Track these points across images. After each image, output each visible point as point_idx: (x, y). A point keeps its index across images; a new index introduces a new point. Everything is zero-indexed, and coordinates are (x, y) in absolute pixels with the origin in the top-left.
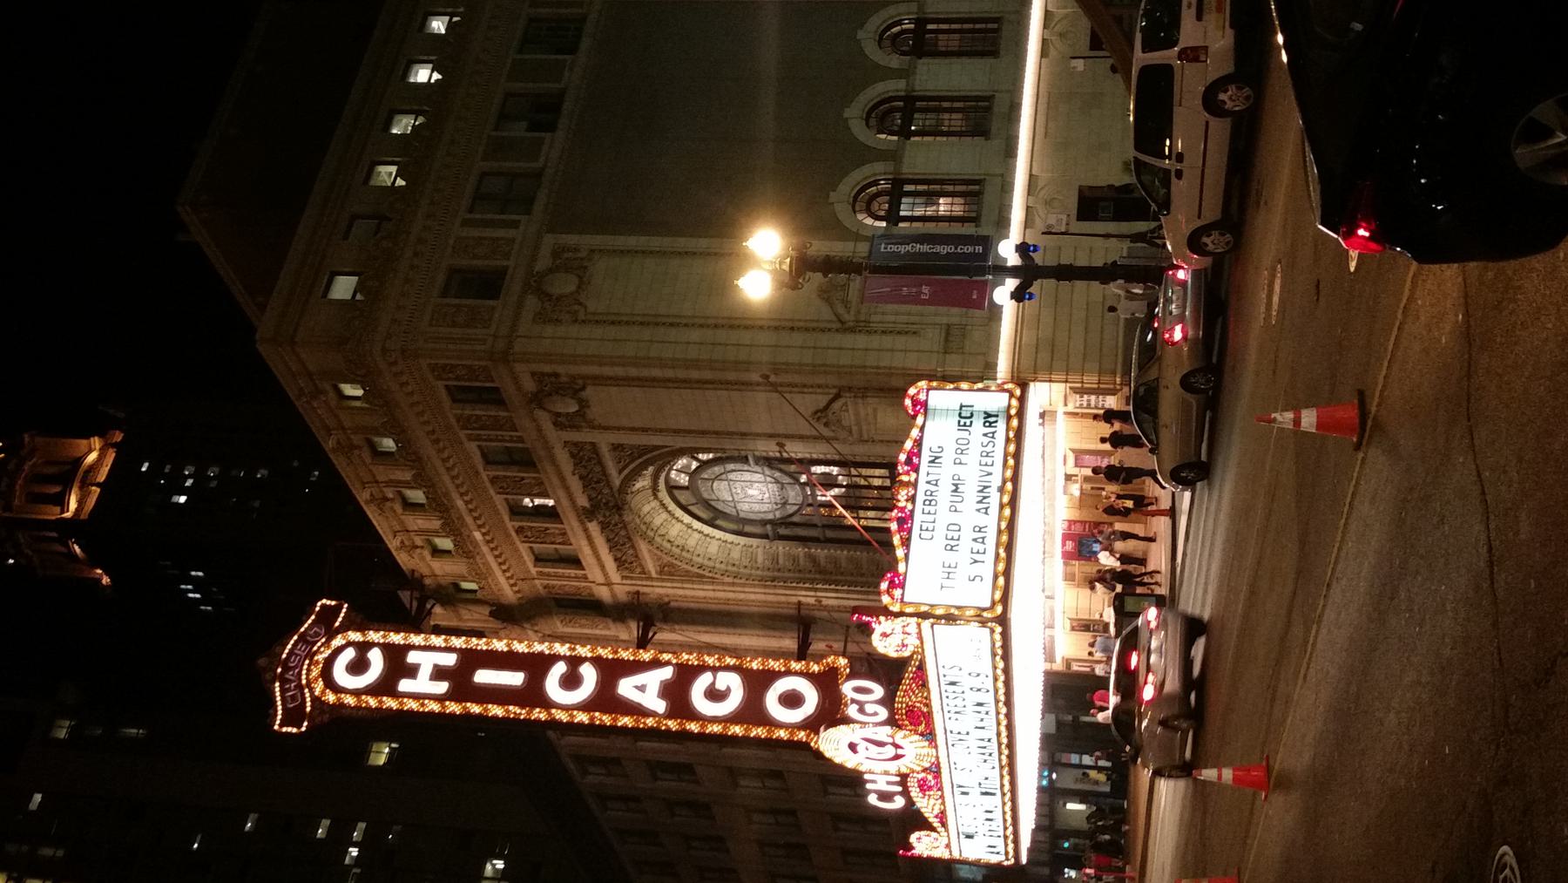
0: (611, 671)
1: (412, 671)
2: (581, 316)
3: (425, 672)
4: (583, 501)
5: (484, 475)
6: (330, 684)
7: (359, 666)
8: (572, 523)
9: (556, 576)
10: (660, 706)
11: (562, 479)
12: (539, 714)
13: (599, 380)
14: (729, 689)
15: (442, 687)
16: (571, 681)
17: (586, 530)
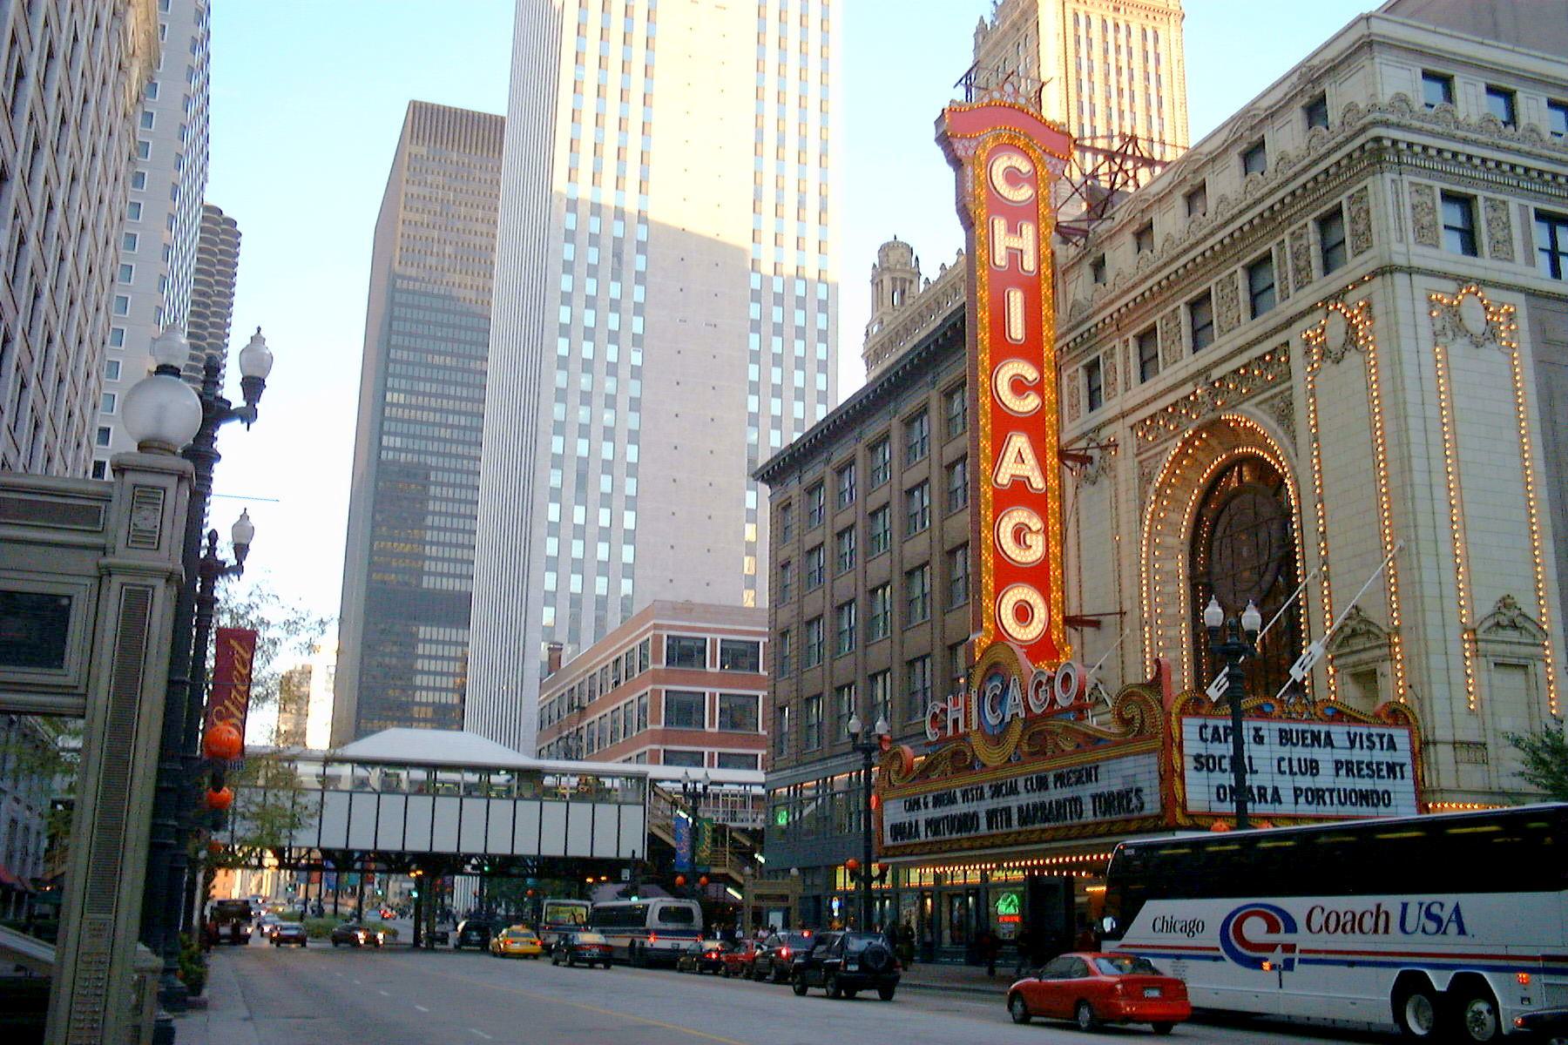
0: (1033, 426)
1: (1013, 229)
2: (1441, 340)
3: (1015, 243)
4: (1216, 374)
5: (1238, 267)
6: (992, 154)
7: (1013, 177)
8: (1190, 363)
10: (1004, 479)
11: (1241, 350)
12: (984, 358)
15: (1001, 259)
16: (1019, 386)
17: (1184, 382)
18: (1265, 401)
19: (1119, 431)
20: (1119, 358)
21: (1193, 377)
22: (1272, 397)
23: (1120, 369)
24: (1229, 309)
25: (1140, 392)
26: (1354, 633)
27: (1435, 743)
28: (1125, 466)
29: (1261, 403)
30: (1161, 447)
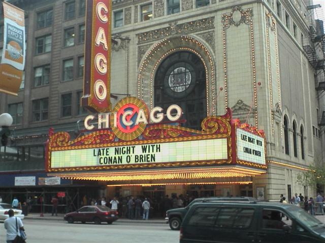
4: (180, 23)
8: (167, 18)
9: (136, 12)
13: (251, 30)
14: (103, 68)
18: (201, 34)
19: (132, 35)
20: (133, 11)
21: (169, 22)
22: (204, 33)
23: (133, 15)
24: (187, 2)
25: (140, 24)
26: (240, 108)
27: (268, 143)
28: (133, 47)
29: (199, 34)
30: (150, 43)
